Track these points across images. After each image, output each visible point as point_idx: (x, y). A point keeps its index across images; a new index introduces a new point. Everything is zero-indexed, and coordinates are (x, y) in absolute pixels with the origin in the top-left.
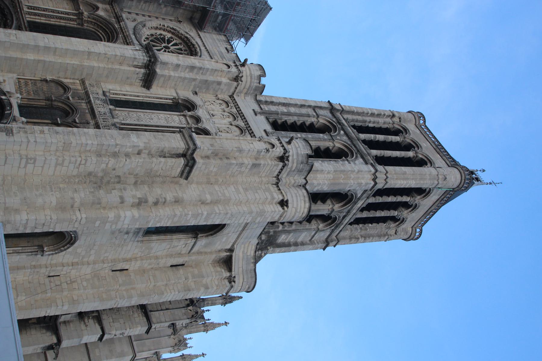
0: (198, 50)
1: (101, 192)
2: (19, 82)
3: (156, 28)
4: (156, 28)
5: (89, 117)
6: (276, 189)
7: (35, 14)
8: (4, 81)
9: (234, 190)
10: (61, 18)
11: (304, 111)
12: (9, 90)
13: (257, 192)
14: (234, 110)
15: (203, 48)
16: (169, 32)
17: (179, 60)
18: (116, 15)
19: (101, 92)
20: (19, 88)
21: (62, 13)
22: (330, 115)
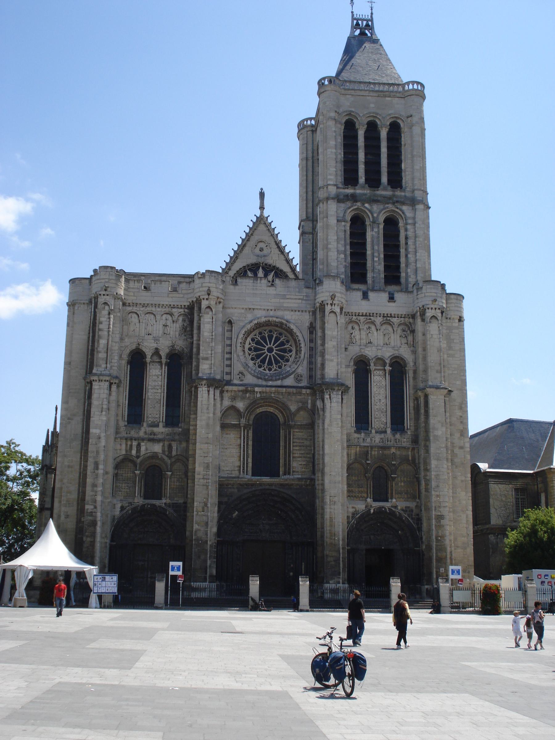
0: (277, 320)
1: (456, 460)
2: (349, 496)
3: (244, 351)
4: (244, 351)
5: (386, 452)
6: (448, 321)
7: (247, 466)
8: (353, 508)
9: (451, 359)
10: (247, 444)
11: (342, 235)
12: (364, 506)
13: (453, 339)
14: (362, 318)
15: (272, 313)
16: (246, 338)
17: (332, 360)
18: (242, 391)
19: (356, 435)
20: (357, 498)
21: (244, 443)
22: (342, 205)
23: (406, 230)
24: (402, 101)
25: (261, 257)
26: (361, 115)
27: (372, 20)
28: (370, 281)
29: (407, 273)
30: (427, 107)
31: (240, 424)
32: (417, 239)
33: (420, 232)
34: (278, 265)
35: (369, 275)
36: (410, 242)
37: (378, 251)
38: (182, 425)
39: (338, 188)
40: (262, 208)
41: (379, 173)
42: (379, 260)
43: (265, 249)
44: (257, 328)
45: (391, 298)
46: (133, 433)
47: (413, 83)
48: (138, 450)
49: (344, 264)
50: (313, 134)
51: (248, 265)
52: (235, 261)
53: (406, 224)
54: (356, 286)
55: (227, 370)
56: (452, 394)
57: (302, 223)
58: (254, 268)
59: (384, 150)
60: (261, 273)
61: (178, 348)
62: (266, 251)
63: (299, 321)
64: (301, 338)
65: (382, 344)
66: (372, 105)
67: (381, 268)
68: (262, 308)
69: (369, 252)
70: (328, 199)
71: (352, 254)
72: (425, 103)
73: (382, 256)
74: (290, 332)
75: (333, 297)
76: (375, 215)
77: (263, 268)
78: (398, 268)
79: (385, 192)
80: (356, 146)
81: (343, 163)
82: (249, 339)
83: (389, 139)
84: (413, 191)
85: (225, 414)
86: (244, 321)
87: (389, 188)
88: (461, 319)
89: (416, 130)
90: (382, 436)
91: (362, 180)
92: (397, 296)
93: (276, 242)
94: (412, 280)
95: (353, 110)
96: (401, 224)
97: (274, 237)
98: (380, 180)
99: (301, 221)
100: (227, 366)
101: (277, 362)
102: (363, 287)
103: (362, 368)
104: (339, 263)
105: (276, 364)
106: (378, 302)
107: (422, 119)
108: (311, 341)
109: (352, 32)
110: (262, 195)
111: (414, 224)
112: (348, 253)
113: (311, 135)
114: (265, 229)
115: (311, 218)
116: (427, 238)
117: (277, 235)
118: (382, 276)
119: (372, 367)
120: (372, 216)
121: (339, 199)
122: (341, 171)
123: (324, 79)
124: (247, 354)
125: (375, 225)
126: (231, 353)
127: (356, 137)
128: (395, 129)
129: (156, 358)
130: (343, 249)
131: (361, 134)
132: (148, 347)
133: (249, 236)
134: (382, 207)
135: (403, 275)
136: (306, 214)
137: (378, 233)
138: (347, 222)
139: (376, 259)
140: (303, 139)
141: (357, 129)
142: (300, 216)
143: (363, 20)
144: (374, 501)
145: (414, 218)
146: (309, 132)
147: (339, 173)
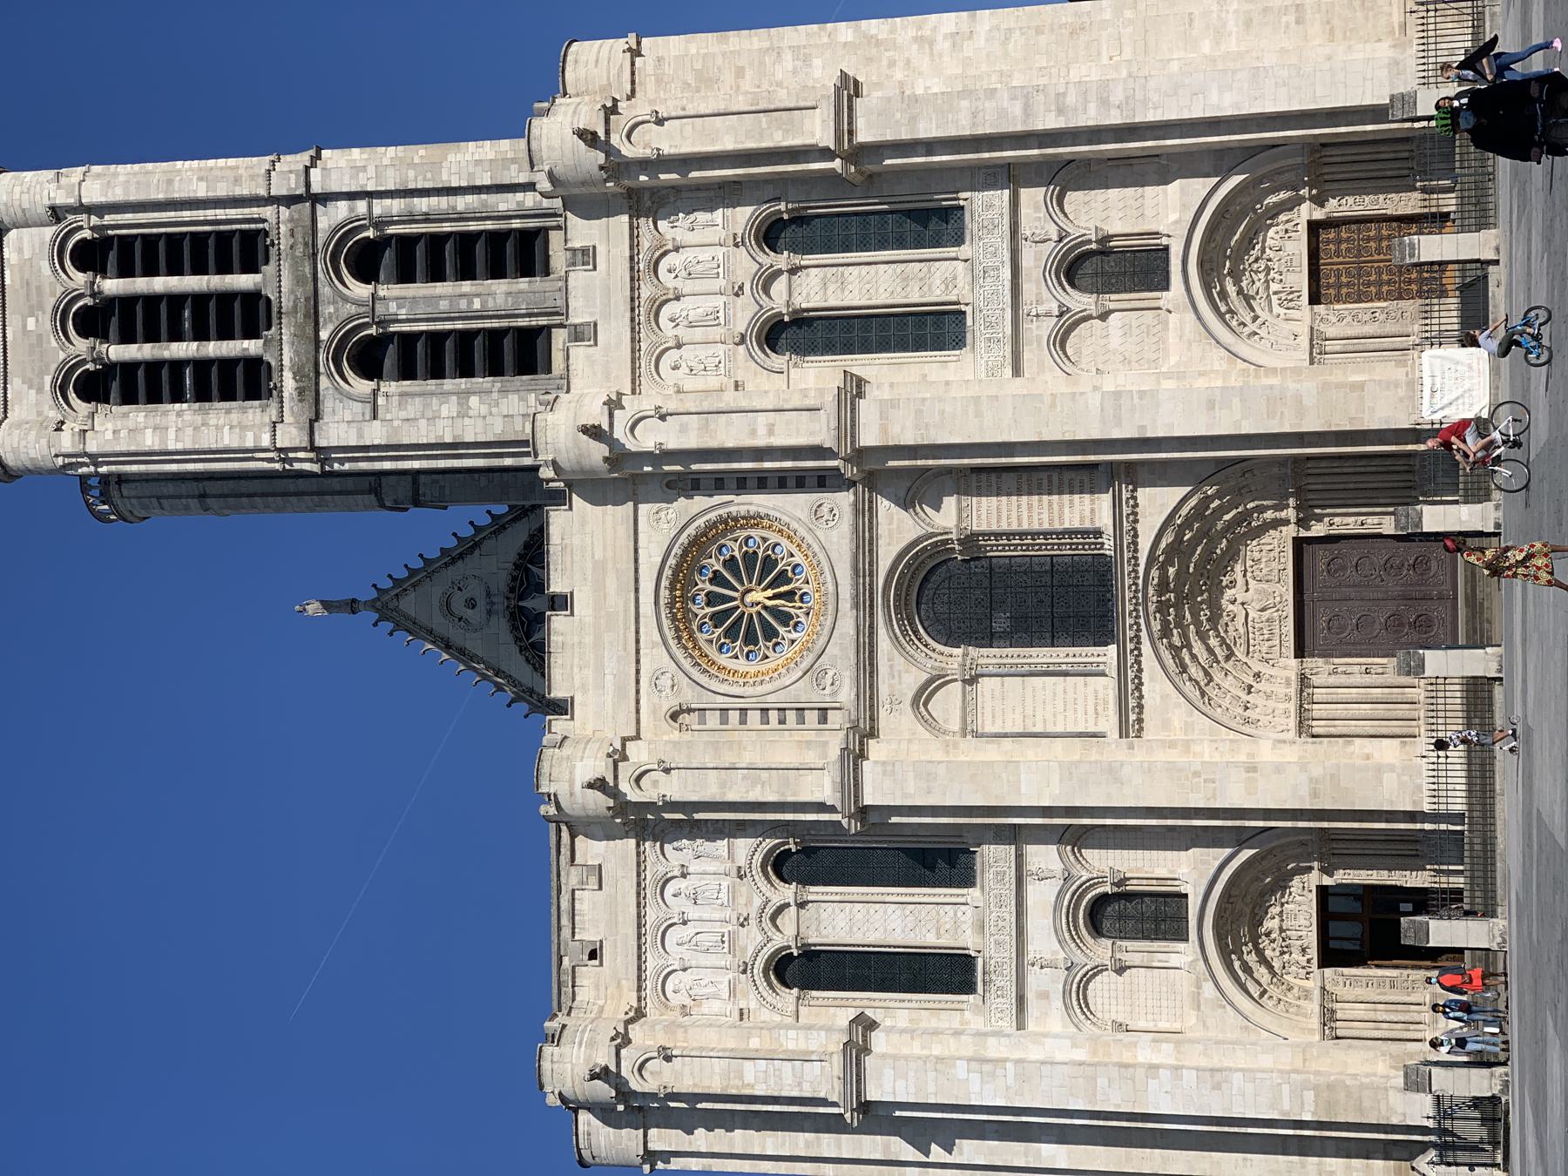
11: (414, 407)
22: (328, 405)
25: (493, 603)
26: (62, 356)
31: (964, 681)
32: (411, 186)
34: (513, 557)
36: (422, 204)
37: (452, 298)
42: (478, 295)
43: (466, 594)
44: (691, 637)
45: (586, 256)
46: (1004, 981)
49: (495, 395)
50: (127, 481)
51: (517, 639)
55: (811, 717)
56: (851, 74)
57: (388, 504)
59: (161, 284)
61: (758, 858)
64: (712, 516)
67: (500, 287)
68: (633, 628)
71: (466, 371)
74: (699, 545)
76: (353, 309)
77: (521, 598)
79: (277, 281)
80: (154, 366)
81: (207, 405)
82: (723, 660)
83: (125, 272)
87: (269, 269)
90: (979, 269)
91: (252, 347)
93: (446, 565)
94: (529, 200)
95: (48, 379)
96: (370, 233)
97: (429, 569)
99: (382, 506)
100: (801, 720)
101: (782, 578)
102: (559, 337)
104: (494, 410)
105: (789, 581)
111: (369, 195)
112: (463, 383)
113: (133, 485)
114: (412, 596)
115: (372, 479)
117: (425, 560)
120: (350, 319)
122: (228, 411)
124: (764, 667)
125: (380, 309)
126: (765, 711)
127: (129, 367)
129: (788, 920)
130: (454, 398)
131: (118, 352)
132: (758, 943)
134: (325, 291)
136: (362, 493)
138: (375, 393)
139: (477, 304)
140: (145, 507)
141: (104, 365)
142: (367, 508)
144: (1167, 288)
145: (352, 196)
146: (125, 493)
147: (234, 416)
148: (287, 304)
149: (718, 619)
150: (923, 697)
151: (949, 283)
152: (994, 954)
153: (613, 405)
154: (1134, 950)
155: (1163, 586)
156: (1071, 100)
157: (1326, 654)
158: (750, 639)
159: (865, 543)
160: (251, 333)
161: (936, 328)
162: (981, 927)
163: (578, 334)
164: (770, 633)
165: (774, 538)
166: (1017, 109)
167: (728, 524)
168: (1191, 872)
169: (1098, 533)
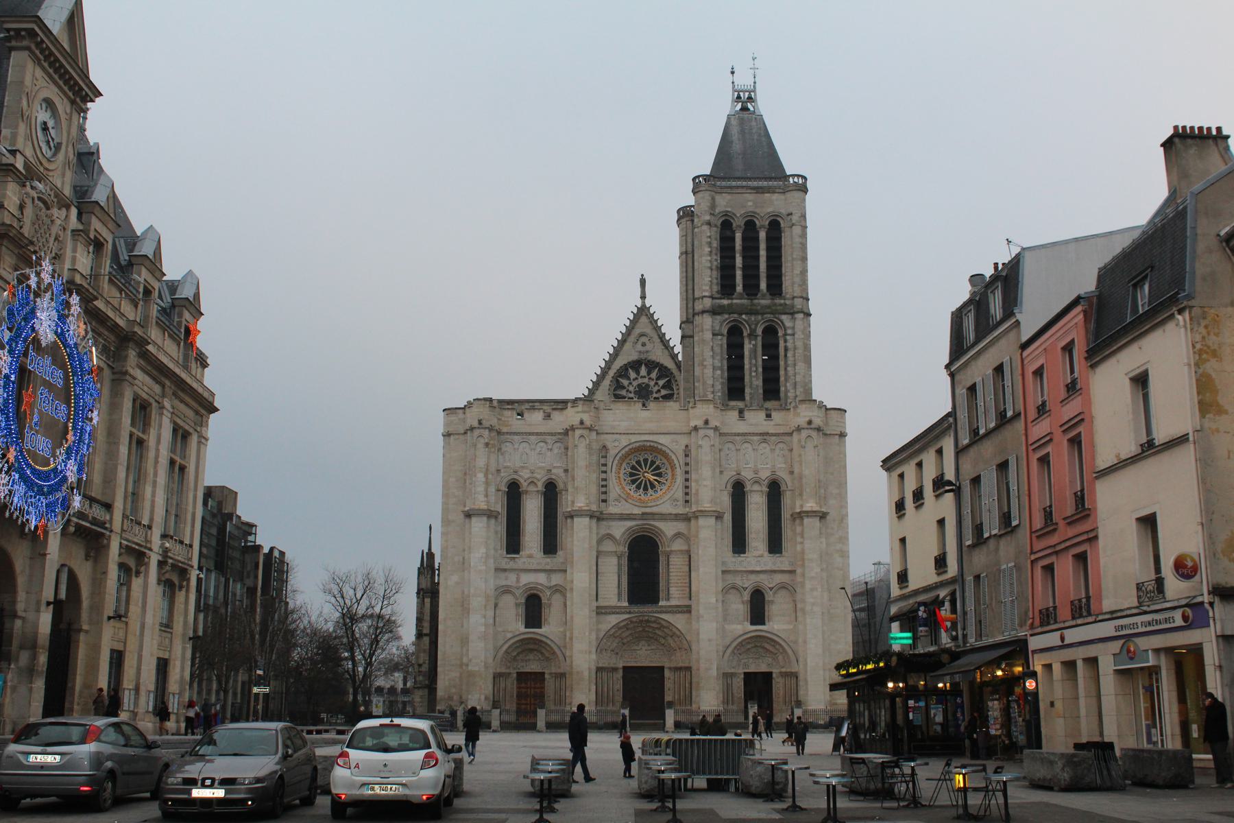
11: (717, 350)
22: (718, 317)
23: (785, 341)
24: (782, 197)
27: (754, 91)
28: (747, 397)
29: (786, 387)
30: (812, 202)
33: (799, 344)
34: (662, 362)
35: (747, 390)
36: (790, 354)
37: (756, 365)
38: (560, 553)
39: (712, 297)
40: (643, 297)
41: (757, 277)
45: (768, 416)
46: (512, 565)
47: (793, 176)
48: (518, 580)
52: (615, 359)
53: (785, 334)
54: (733, 403)
55: (603, 497)
58: (635, 365)
59: (763, 253)
60: (643, 371)
62: (649, 347)
63: (673, 445)
65: (758, 464)
66: (750, 204)
67: (760, 382)
69: (747, 367)
70: (703, 312)
71: (729, 368)
72: (807, 197)
73: (760, 370)
75: (706, 422)
78: (777, 380)
82: (624, 465)
83: (768, 239)
84: (794, 298)
85: (600, 542)
86: (617, 445)
87: (768, 296)
88: (842, 435)
89: (797, 230)
91: (739, 288)
92: (774, 414)
96: (780, 333)
97: (657, 329)
98: (758, 286)
102: (740, 404)
103: (738, 492)
106: (756, 420)
107: (804, 216)
108: (687, 464)
109: (733, 107)
110: (643, 282)
116: (807, 348)
118: (761, 391)
119: (748, 488)
121: (714, 312)
123: (698, 177)
127: (733, 239)
128: (775, 227)
131: (738, 236)
133: (630, 330)
135: (782, 389)
137: (755, 346)
143: (744, 91)
145: (793, 328)
148: (756, 301)
149: (638, 462)
150: (610, 536)
151: (756, 549)
152: (521, 561)
153: (716, 429)
154: (522, 610)
155: (648, 621)
156: (815, 593)
157: (624, 677)
158: (632, 475)
159: (664, 517)
160: (744, 286)
161: (739, 544)
162: (530, 556)
163: (741, 412)
164: (633, 482)
165: (668, 484)
166: (813, 574)
167: (673, 468)
168: (549, 630)
169: (668, 599)
